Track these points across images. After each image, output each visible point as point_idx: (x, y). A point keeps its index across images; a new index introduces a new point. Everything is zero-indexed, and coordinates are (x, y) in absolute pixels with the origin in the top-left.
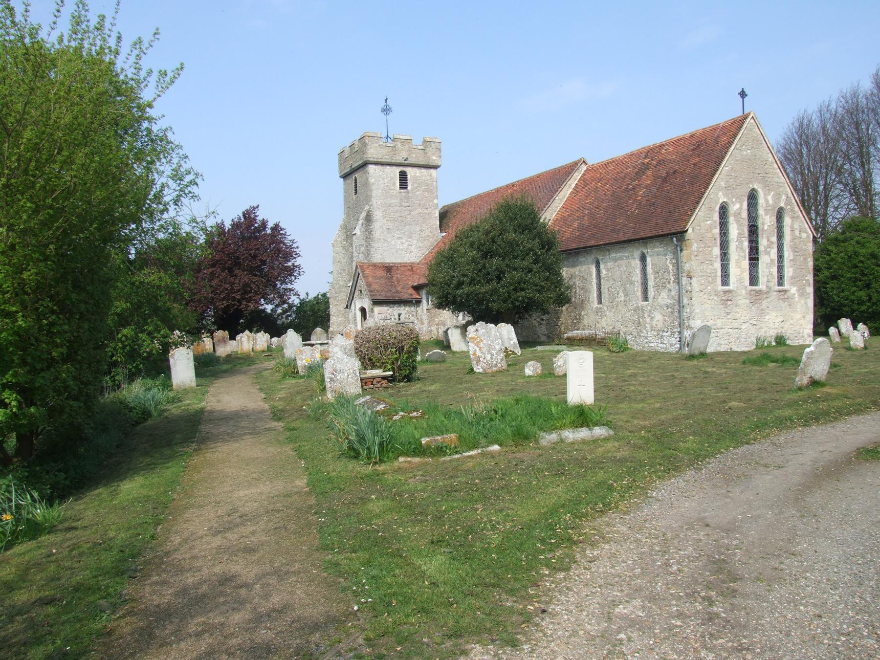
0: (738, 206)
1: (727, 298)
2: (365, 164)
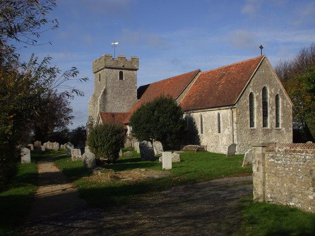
0: (258, 94)
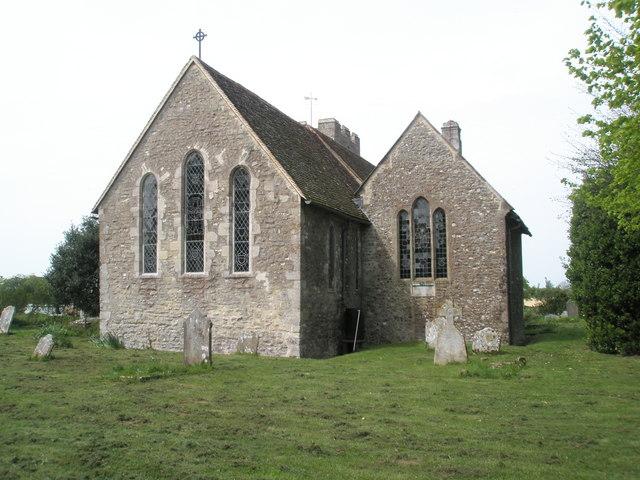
0: (167, 175)
1: (149, 290)
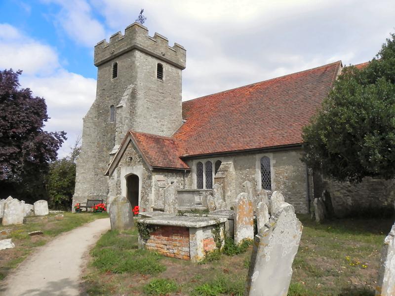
2: (134, 48)
